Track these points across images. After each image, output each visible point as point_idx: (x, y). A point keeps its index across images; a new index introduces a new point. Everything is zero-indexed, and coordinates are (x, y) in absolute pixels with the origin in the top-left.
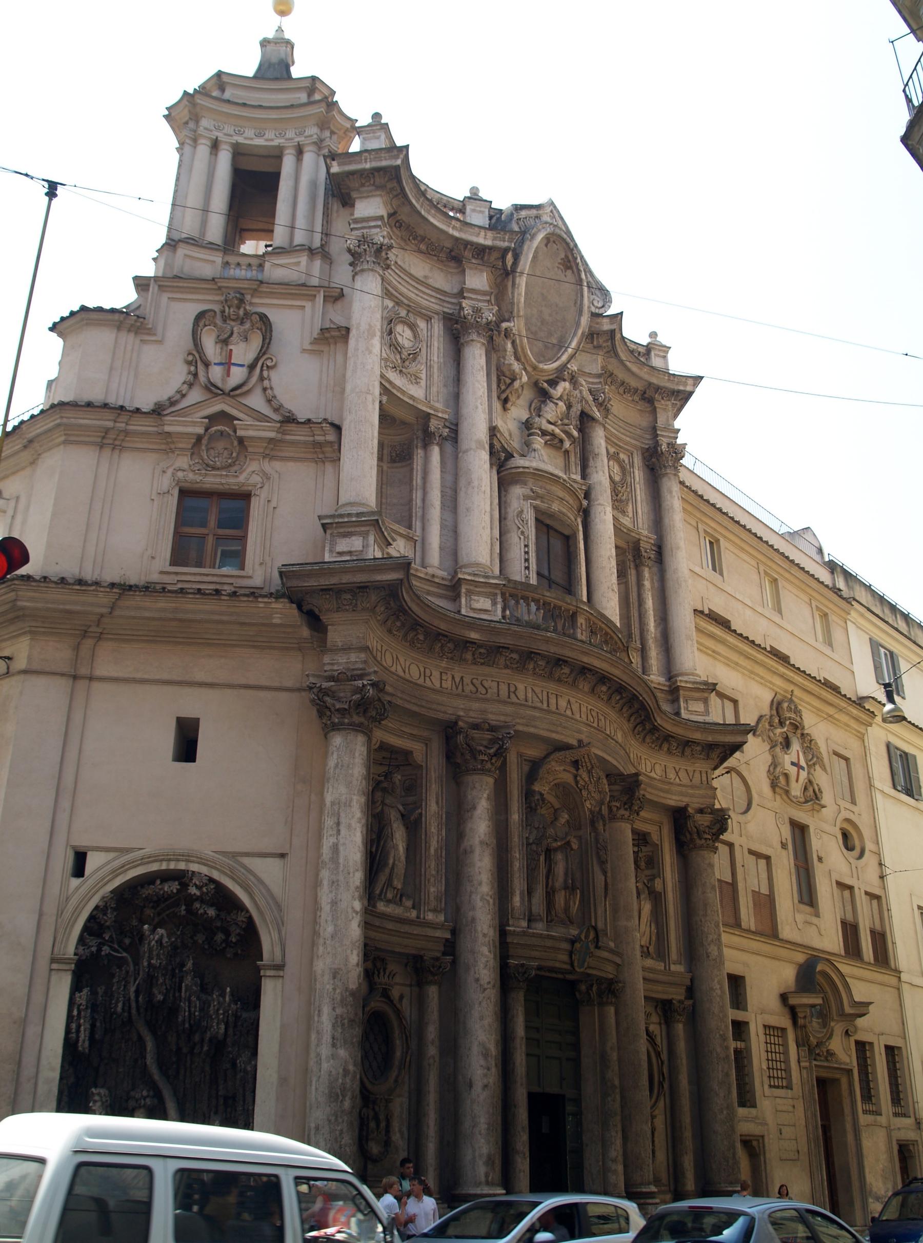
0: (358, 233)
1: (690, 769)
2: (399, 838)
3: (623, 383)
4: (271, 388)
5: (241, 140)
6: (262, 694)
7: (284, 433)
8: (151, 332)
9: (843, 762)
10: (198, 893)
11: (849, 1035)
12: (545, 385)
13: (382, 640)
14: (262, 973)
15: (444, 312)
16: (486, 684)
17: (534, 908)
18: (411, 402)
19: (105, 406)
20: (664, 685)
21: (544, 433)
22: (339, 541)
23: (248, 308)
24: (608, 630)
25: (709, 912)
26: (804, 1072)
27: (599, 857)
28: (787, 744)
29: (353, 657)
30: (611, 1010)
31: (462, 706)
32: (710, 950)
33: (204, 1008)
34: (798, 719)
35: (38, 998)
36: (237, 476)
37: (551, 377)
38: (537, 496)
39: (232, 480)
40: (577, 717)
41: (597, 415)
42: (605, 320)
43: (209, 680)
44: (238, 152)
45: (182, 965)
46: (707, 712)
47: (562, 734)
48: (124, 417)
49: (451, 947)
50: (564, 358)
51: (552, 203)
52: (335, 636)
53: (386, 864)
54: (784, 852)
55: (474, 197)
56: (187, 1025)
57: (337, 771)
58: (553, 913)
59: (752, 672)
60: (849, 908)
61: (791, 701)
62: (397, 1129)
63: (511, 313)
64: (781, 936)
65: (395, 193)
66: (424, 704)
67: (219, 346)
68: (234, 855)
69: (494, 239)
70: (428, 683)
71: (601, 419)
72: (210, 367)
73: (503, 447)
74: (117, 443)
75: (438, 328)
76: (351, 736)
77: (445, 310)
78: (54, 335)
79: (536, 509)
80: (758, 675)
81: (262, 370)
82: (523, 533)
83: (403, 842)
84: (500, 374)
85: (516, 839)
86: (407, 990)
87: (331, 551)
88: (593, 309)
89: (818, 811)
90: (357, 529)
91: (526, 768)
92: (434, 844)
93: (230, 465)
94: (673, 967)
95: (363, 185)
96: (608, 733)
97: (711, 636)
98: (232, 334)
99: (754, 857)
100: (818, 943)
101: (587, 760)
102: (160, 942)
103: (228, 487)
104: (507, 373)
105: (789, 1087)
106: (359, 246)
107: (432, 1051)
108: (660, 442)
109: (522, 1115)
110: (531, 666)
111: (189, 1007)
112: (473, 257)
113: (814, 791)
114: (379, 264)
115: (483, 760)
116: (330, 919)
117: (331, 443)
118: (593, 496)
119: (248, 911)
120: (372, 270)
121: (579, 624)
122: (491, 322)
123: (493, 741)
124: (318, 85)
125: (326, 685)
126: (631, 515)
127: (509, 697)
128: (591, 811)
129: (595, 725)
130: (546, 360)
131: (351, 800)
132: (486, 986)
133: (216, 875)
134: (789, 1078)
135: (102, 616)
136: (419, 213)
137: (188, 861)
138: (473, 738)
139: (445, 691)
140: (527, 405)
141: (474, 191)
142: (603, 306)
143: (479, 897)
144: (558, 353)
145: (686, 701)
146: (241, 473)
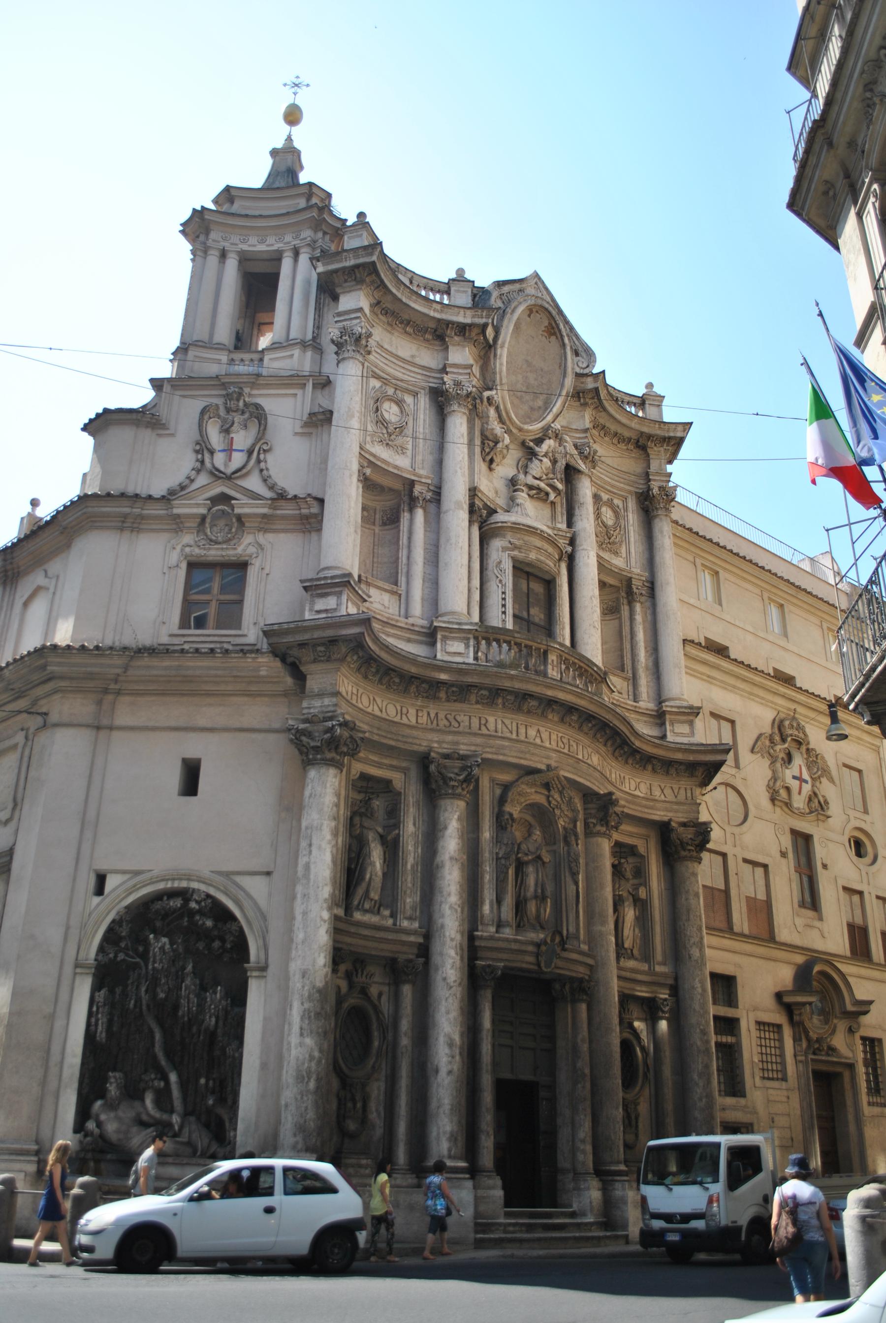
0: (340, 325)
1: (675, 787)
2: (376, 856)
3: (616, 434)
4: (267, 469)
5: (245, 247)
6: (254, 736)
7: (275, 509)
8: (164, 426)
9: (855, 775)
10: (197, 907)
11: (853, 1032)
12: (531, 444)
13: (357, 685)
14: (249, 974)
15: (430, 387)
16: (458, 718)
17: (502, 915)
18: (396, 471)
19: (123, 495)
20: (652, 710)
21: (531, 487)
22: (317, 600)
23: (247, 399)
24: (582, 664)
25: (691, 916)
26: (801, 1066)
27: (570, 868)
28: (789, 758)
29: (327, 701)
30: (584, 1006)
31: (436, 739)
32: (692, 952)
33: (201, 1005)
34: (801, 735)
35: (64, 996)
36: (235, 549)
37: (537, 436)
38: (516, 547)
39: (231, 552)
40: (547, 745)
41: (582, 466)
42: (589, 379)
43: (209, 725)
44: (244, 259)
45: (184, 968)
46: (692, 734)
47: (530, 760)
48: (138, 505)
49: (425, 951)
50: (550, 418)
51: (536, 275)
52: (313, 683)
53: (363, 879)
54: (784, 861)
55: (460, 279)
56: (186, 1019)
57: (311, 800)
58: (525, 919)
59: (751, 694)
60: (858, 912)
61: (794, 718)
62: (374, 1109)
63: (494, 382)
64: (777, 939)
65: (376, 285)
66: (400, 738)
67: (222, 435)
68: (228, 875)
69: (473, 317)
70: (405, 720)
71: (586, 471)
72: (215, 455)
73: (485, 505)
74: (135, 525)
75: (424, 401)
76: (323, 770)
77: (431, 385)
78: (85, 434)
79: (514, 560)
80: (758, 696)
81: (259, 454)
82: (501, 581)
84: (484, 437)
85: (487, 855)
86: (385, 989)
87: (311, 610)
88: (578, 370)
89: (823, 821)
90: (333, 590)
91: (498, 791)
92: (411, 861)
93: (230, 540)
94: (659, 969)
95: (346, 281)
96: (580, 757)
97: (704, 663)
98: (233, 423)
99: (750, 866)
100: (819, 945)
102: (162, 949)
103: (227, 558)
104: (491, 437)
105: (784, 1079)
106: (341, 337)
107: (405, 1041)
108: (652, 486)
109: (487, 1098)
110: (500, 701)
111: (188, 1003)
112: (456, 334)
113: (819, 802)
114: (358, 351)
115: (453, 786)
116: (301, 926)
117: (315, 514)
118: (578, 542)
119: (239, 922)
120: (352, 358)
121: (550, 661)
122: (471, 393)
123: (463, 769)
124: (314, 190)
125: (302, 726)
126: (624, 555)
127: (480, 729)
128: (565, 828)
129: (566, 751)
130: (532, 421)
131: (322, 825)
132: (452, 984)
133: (212, 892)
134: (784, 1071)
135: (118, 675)
136: (400, 301)
137: (189, 880)
138: (445, 767)
139: (420, 726)
140: (515, 463)
141: (460, 272)
142: (588, 366)
143: (447, 907)
144: (544, 413)
145: (672, 724)
146: (239, 546)
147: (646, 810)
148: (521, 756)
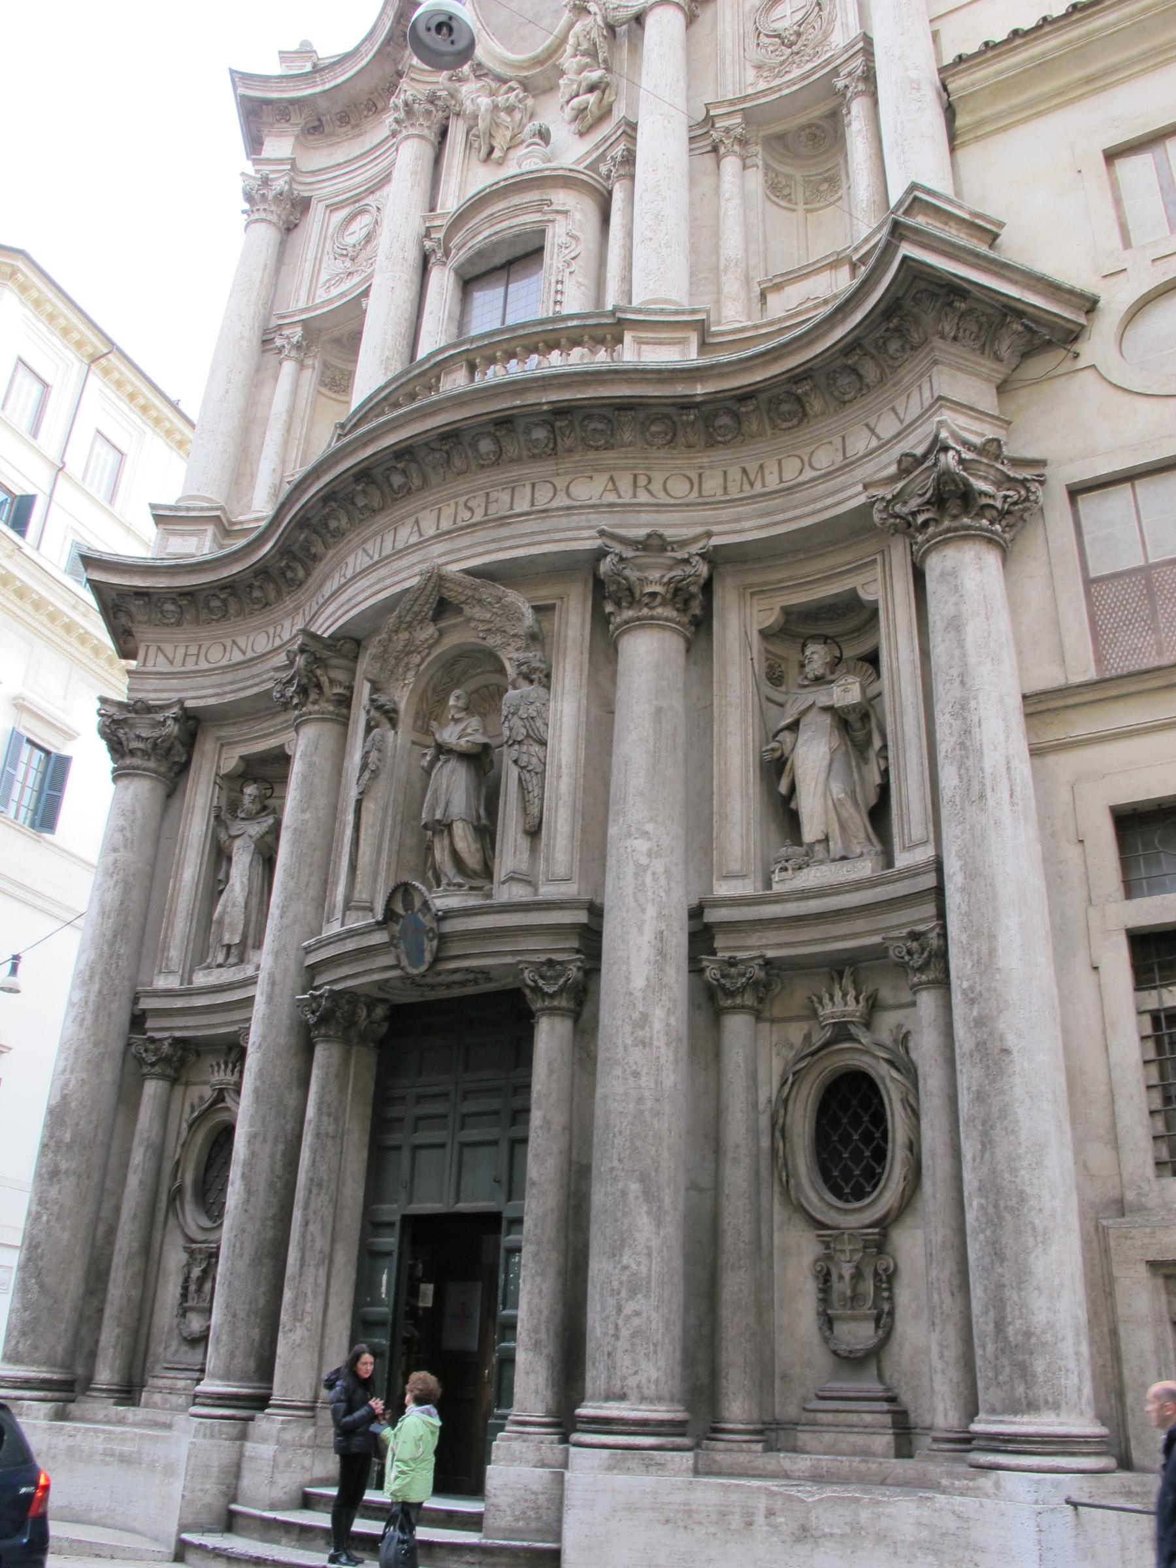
13: (195, 640)
83: (242, 876)
101: (460, 590)
147: (829, 501)
148: (377, 587)
